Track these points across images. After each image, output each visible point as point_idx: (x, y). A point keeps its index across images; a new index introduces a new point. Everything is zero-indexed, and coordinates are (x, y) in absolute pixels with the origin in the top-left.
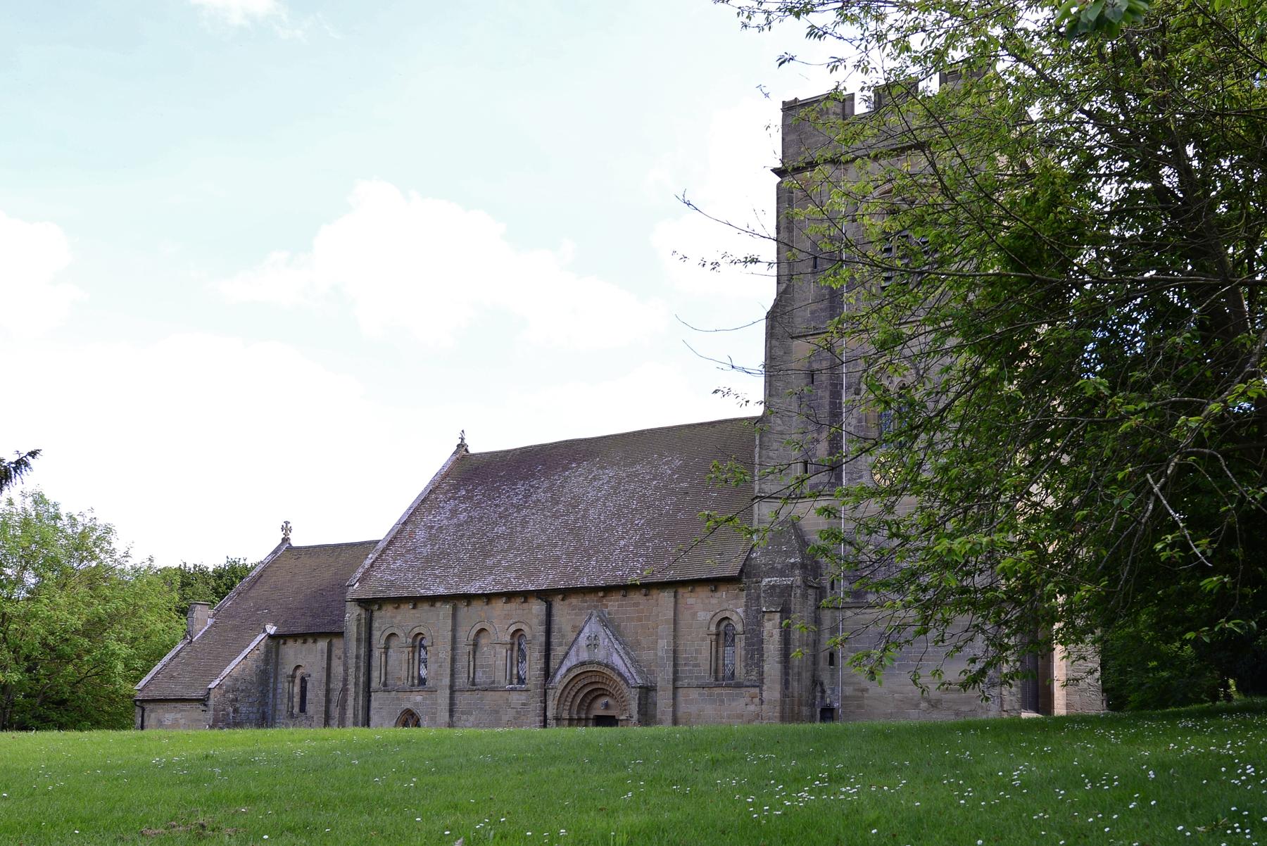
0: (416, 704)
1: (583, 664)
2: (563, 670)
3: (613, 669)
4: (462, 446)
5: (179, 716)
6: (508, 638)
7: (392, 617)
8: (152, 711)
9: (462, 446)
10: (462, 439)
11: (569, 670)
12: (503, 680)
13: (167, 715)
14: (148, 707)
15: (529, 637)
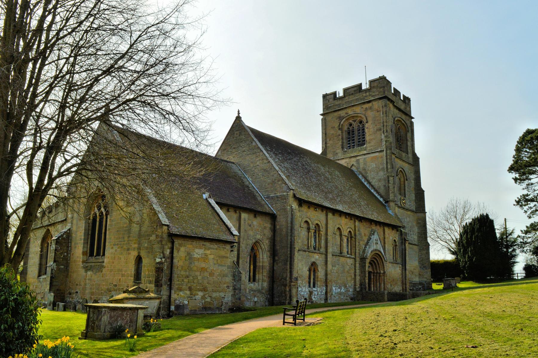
0: (316, 259)
1: (376, 250)
2: (370, 252)
3: (382, 254)
4: (238, 118)
5: (208, 252)
6: (347, 234)
7: (306, 212)
8: (180, 245)
9: (238, 118)
10: (239, 113)
11: (371, 252)
12: (346, 253)
13: (197, 250)
14: (177, 242)
15: (353, 235)
